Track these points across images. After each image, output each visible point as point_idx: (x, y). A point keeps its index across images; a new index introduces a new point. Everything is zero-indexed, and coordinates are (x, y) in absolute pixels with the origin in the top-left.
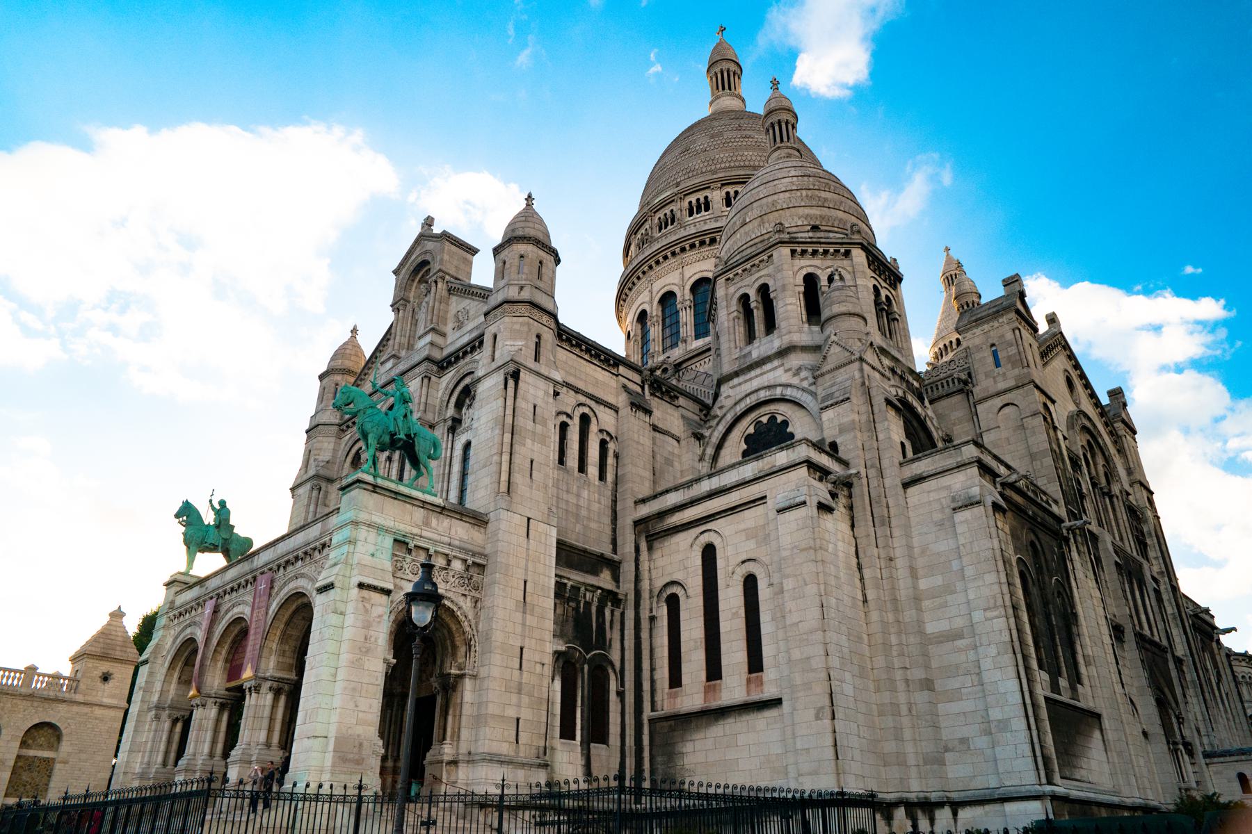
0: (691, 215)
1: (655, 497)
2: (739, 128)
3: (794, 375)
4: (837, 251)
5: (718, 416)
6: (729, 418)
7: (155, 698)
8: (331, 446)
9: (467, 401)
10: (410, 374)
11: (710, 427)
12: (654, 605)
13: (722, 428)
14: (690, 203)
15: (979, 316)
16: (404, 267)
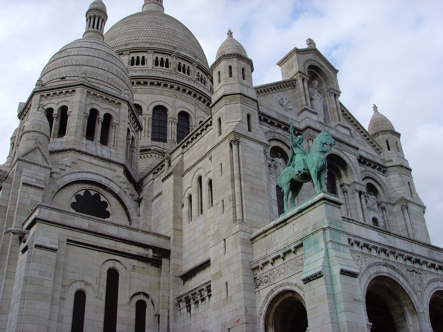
14: (198, 73)
16: (303, 54)
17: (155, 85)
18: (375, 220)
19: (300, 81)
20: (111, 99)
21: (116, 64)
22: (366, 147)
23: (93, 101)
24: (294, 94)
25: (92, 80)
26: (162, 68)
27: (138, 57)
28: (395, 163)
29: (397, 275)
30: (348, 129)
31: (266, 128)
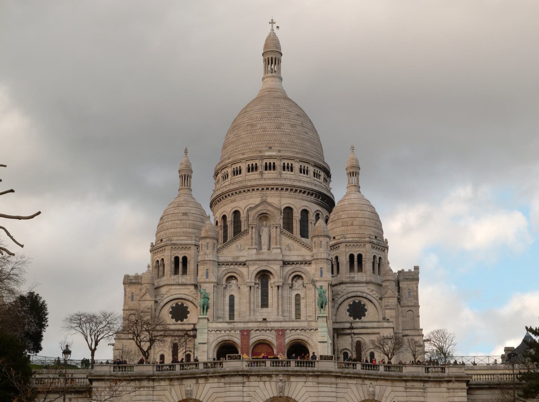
0: (284, 169)
1: (341, 323)
2: (302, 125)
3: (371, 291)
4: (382, 249)
5: (340, 295)
6: (345, 297)
7: (211, 356)
8: (217, 270)
9: (295, 279)
10: (272, 262)
11: (337, 297)
12: (339, 354)
13: (342, 299)
14: (284, 164)
15: (406, 277)
16: (254, 209)
17: (246, 192)
18: (298, 295)
19: (250, 228)
20: (184, 247)
21: (188, 219)
22: (301, 250)
23: (175, 252)
24: (248, 237)
25: (175, 238)
26: (252, 173)
27: (237, 168)
28: (315, 257)
29: (233, 338)
30: (281, 248)
31: (223, 268)
